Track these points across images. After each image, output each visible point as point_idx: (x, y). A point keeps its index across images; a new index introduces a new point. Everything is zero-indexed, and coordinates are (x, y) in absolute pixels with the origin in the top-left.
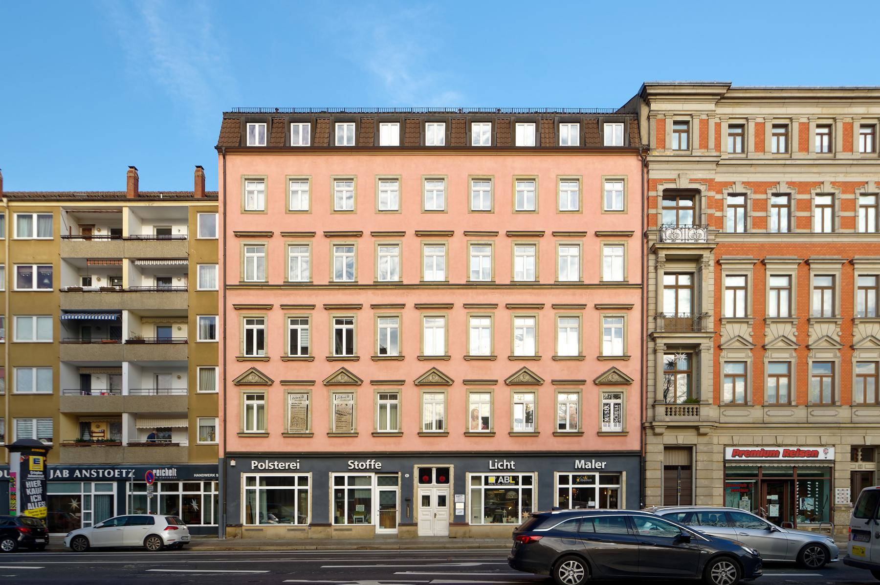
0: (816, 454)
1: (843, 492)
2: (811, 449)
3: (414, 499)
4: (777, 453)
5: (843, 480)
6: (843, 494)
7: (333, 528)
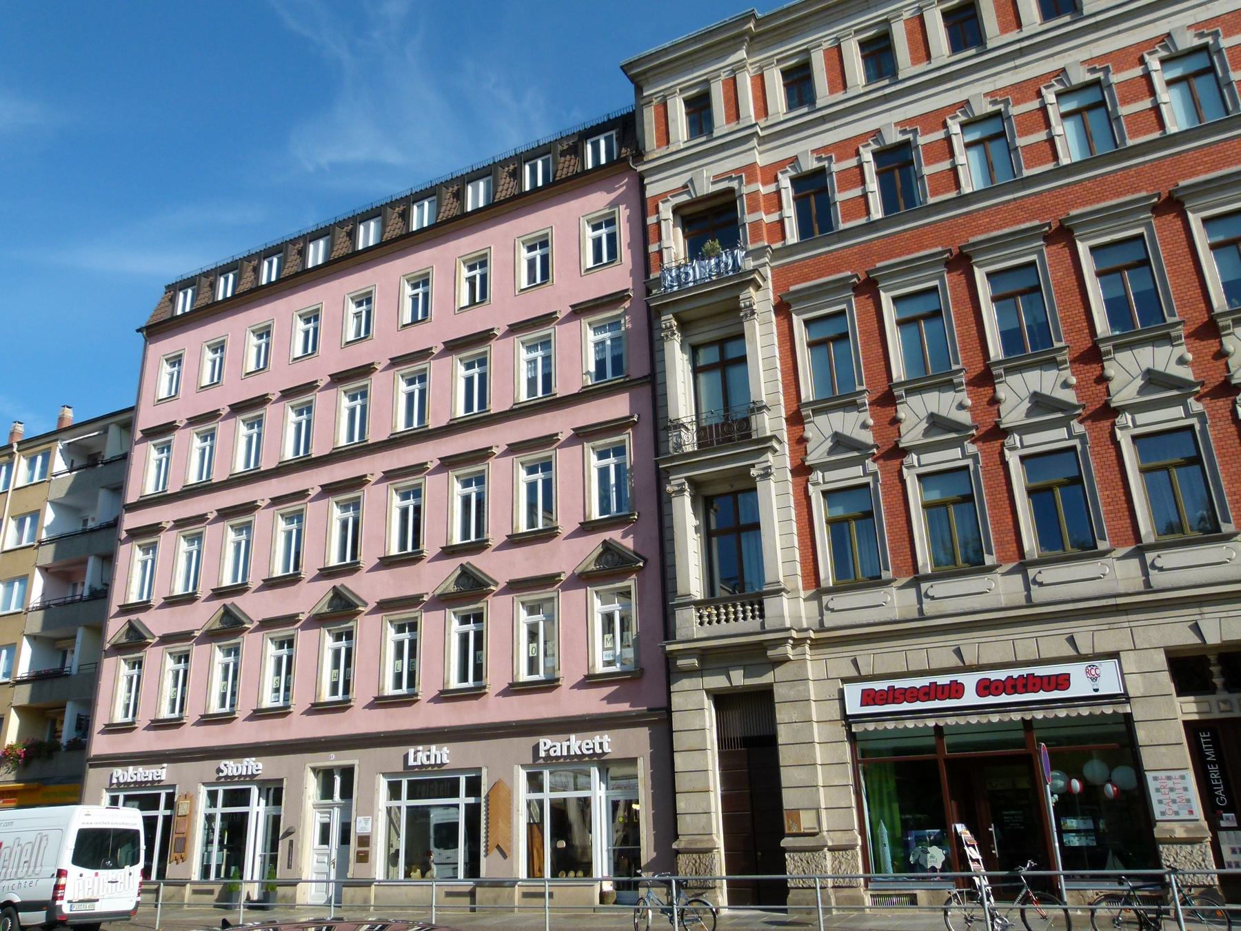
0: (1062, 682)
1: (1170, 784)
2: (943, 680)
3: (300, 830)
4: (956, 690)
5: (1163, 749)
6: (1172, 790)
7: (517, 891)
